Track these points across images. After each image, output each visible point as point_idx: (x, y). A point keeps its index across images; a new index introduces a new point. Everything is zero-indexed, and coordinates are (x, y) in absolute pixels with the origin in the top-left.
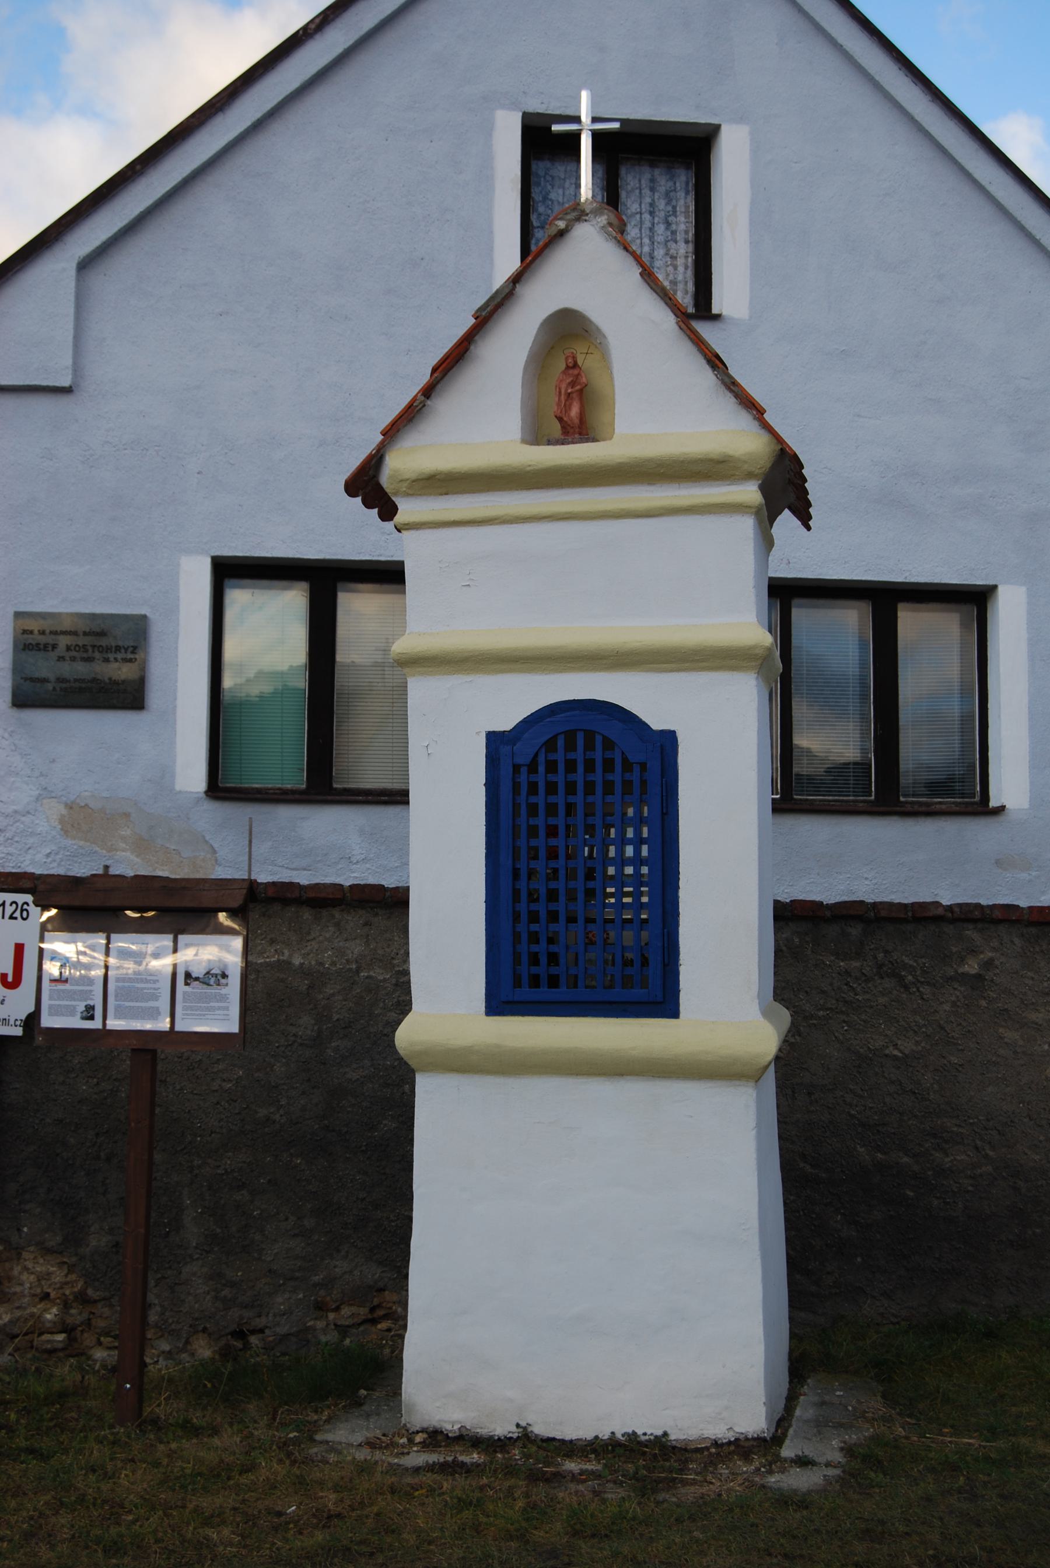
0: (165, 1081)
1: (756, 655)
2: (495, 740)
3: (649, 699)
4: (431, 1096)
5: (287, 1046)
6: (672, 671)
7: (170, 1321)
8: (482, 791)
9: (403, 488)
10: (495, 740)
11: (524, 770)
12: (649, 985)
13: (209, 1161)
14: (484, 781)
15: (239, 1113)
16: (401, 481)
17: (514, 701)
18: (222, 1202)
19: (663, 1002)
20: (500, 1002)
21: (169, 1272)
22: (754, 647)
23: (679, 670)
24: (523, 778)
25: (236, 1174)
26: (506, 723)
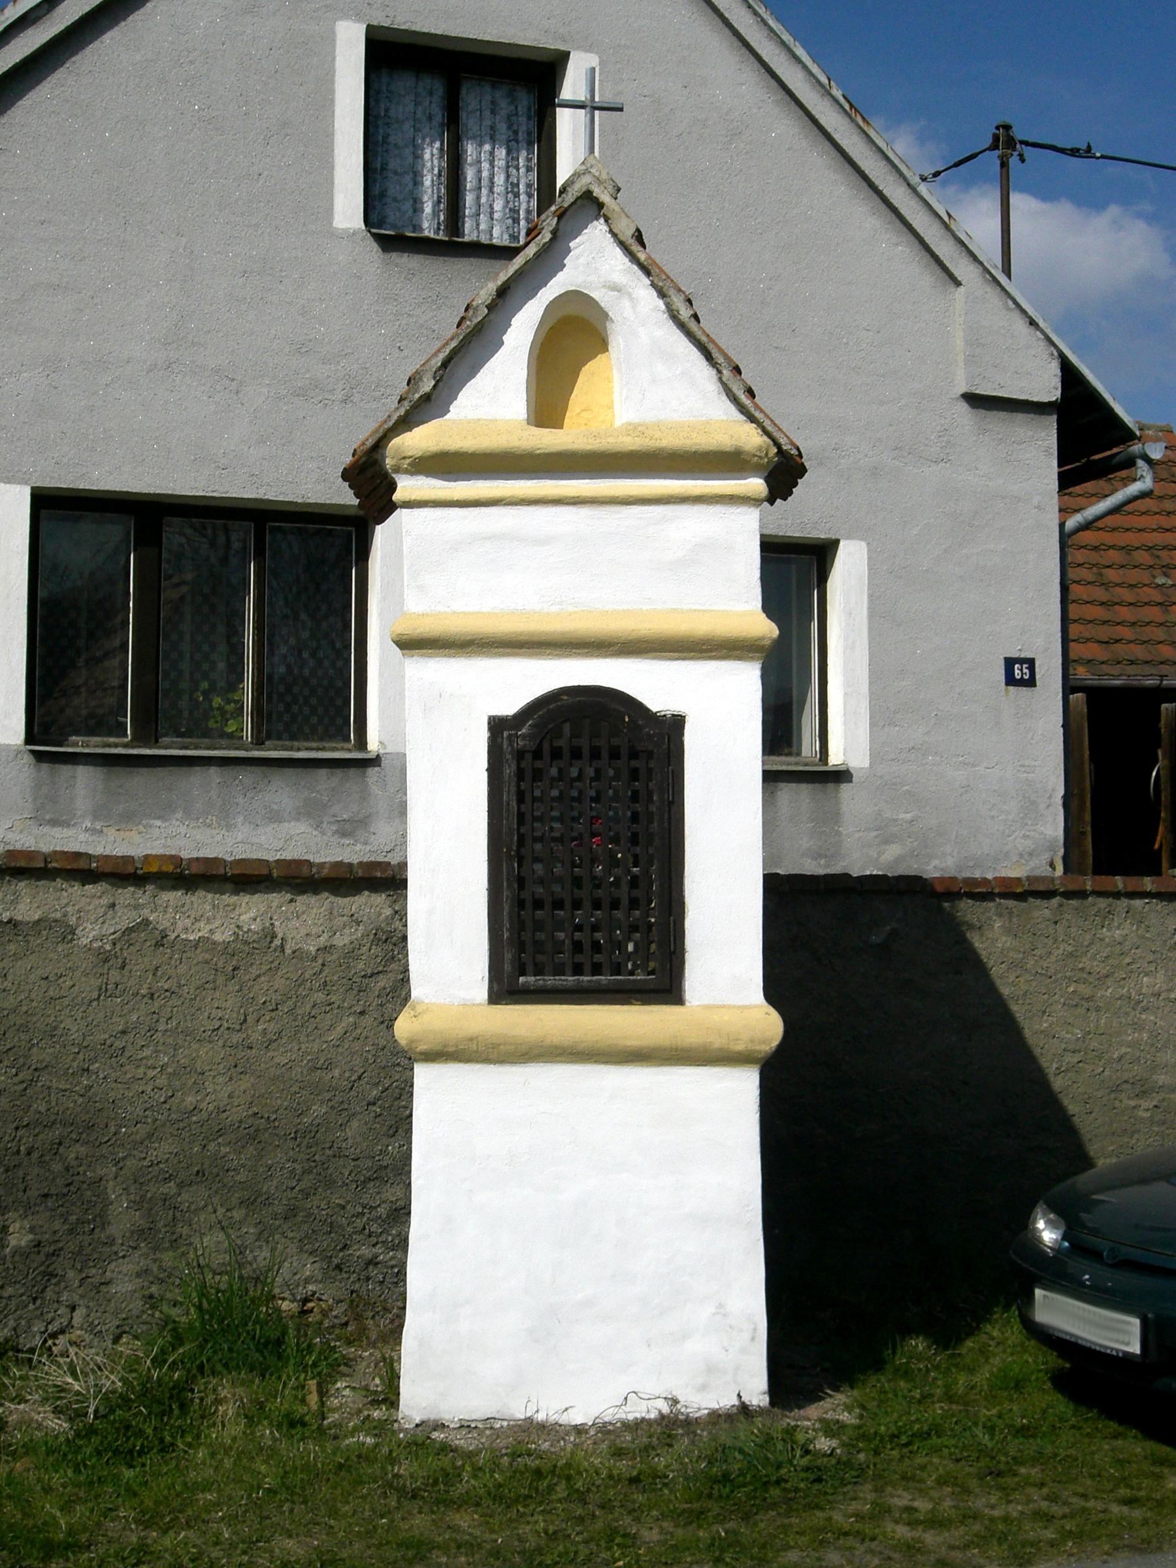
0: (88, 1070)
1: (763, 646)
2: (497, 725)
3: (652, 685)
4: (430, 1085)
5: (214, 1031)
6: (677, 659)
7: (96, 1322)
8: (484, 777)
9: (405, 464)
10: (497, 725)
11: (529, 756)
12: (657, 972)
13: (135, 1152)
14: (486, 766)
15: (165, 1102)
16: (404, 458)
17: (520, 684)
18: (149, 1195)
19: (667, 987)
20: (506, 987)
21: (94, 1271)
22: (763, 638)
23: (684, 659)
24: (526, 764)
25: (161, 1166)
26: (509, 708)
